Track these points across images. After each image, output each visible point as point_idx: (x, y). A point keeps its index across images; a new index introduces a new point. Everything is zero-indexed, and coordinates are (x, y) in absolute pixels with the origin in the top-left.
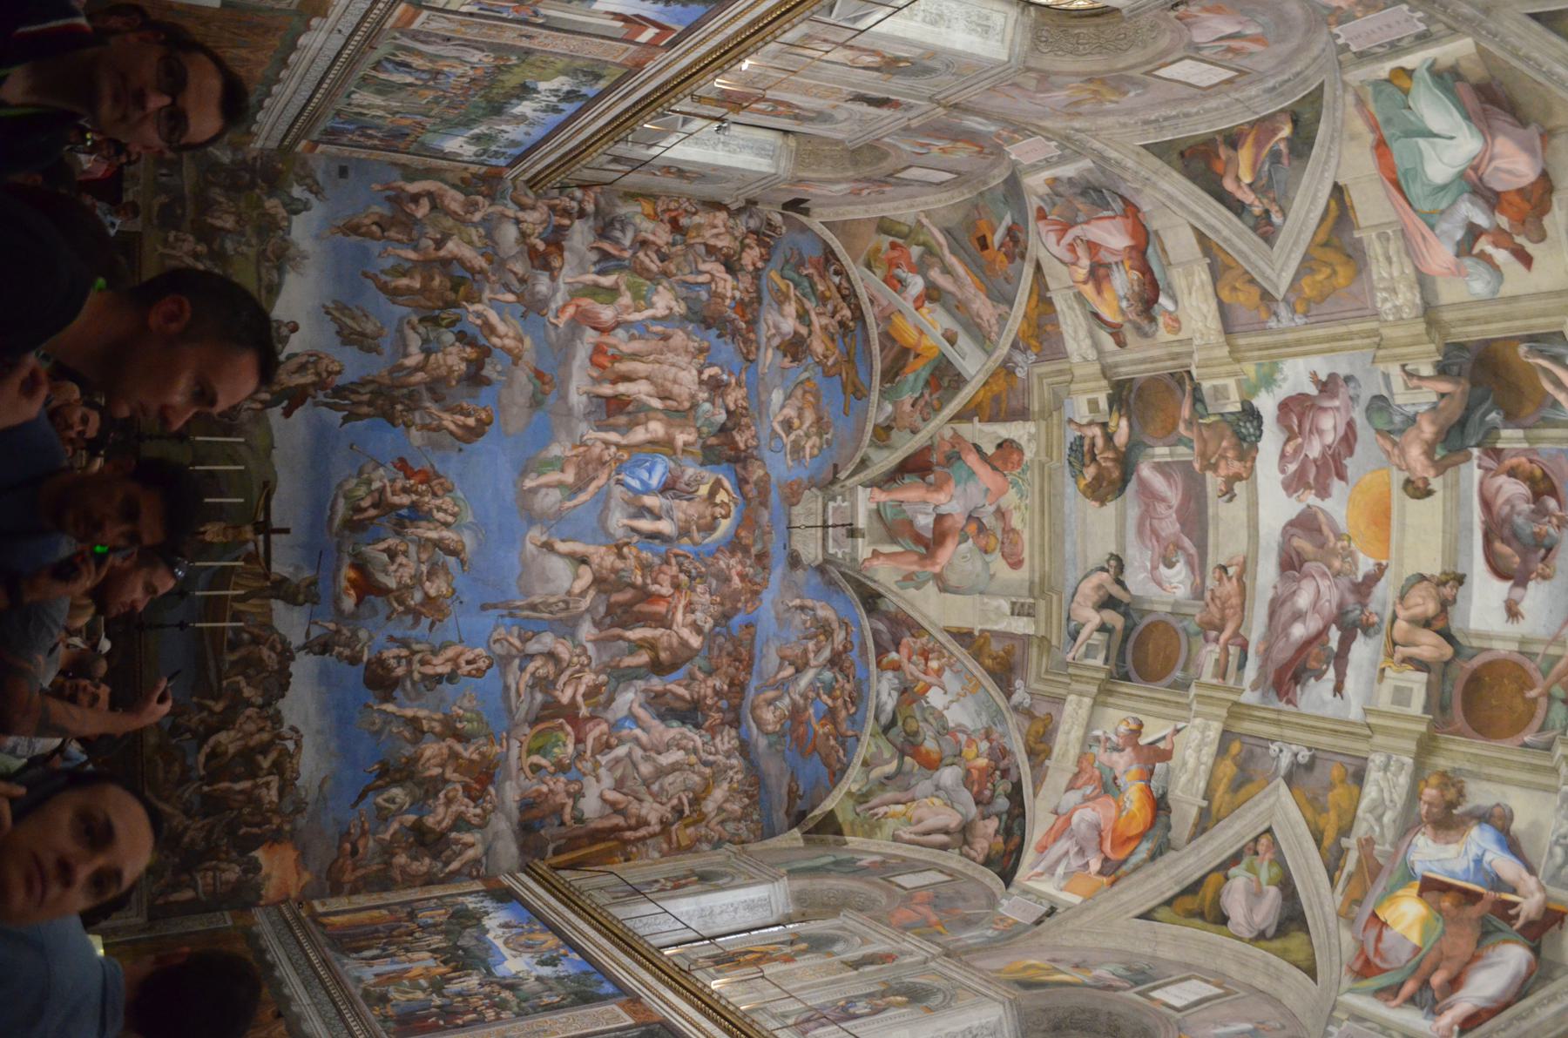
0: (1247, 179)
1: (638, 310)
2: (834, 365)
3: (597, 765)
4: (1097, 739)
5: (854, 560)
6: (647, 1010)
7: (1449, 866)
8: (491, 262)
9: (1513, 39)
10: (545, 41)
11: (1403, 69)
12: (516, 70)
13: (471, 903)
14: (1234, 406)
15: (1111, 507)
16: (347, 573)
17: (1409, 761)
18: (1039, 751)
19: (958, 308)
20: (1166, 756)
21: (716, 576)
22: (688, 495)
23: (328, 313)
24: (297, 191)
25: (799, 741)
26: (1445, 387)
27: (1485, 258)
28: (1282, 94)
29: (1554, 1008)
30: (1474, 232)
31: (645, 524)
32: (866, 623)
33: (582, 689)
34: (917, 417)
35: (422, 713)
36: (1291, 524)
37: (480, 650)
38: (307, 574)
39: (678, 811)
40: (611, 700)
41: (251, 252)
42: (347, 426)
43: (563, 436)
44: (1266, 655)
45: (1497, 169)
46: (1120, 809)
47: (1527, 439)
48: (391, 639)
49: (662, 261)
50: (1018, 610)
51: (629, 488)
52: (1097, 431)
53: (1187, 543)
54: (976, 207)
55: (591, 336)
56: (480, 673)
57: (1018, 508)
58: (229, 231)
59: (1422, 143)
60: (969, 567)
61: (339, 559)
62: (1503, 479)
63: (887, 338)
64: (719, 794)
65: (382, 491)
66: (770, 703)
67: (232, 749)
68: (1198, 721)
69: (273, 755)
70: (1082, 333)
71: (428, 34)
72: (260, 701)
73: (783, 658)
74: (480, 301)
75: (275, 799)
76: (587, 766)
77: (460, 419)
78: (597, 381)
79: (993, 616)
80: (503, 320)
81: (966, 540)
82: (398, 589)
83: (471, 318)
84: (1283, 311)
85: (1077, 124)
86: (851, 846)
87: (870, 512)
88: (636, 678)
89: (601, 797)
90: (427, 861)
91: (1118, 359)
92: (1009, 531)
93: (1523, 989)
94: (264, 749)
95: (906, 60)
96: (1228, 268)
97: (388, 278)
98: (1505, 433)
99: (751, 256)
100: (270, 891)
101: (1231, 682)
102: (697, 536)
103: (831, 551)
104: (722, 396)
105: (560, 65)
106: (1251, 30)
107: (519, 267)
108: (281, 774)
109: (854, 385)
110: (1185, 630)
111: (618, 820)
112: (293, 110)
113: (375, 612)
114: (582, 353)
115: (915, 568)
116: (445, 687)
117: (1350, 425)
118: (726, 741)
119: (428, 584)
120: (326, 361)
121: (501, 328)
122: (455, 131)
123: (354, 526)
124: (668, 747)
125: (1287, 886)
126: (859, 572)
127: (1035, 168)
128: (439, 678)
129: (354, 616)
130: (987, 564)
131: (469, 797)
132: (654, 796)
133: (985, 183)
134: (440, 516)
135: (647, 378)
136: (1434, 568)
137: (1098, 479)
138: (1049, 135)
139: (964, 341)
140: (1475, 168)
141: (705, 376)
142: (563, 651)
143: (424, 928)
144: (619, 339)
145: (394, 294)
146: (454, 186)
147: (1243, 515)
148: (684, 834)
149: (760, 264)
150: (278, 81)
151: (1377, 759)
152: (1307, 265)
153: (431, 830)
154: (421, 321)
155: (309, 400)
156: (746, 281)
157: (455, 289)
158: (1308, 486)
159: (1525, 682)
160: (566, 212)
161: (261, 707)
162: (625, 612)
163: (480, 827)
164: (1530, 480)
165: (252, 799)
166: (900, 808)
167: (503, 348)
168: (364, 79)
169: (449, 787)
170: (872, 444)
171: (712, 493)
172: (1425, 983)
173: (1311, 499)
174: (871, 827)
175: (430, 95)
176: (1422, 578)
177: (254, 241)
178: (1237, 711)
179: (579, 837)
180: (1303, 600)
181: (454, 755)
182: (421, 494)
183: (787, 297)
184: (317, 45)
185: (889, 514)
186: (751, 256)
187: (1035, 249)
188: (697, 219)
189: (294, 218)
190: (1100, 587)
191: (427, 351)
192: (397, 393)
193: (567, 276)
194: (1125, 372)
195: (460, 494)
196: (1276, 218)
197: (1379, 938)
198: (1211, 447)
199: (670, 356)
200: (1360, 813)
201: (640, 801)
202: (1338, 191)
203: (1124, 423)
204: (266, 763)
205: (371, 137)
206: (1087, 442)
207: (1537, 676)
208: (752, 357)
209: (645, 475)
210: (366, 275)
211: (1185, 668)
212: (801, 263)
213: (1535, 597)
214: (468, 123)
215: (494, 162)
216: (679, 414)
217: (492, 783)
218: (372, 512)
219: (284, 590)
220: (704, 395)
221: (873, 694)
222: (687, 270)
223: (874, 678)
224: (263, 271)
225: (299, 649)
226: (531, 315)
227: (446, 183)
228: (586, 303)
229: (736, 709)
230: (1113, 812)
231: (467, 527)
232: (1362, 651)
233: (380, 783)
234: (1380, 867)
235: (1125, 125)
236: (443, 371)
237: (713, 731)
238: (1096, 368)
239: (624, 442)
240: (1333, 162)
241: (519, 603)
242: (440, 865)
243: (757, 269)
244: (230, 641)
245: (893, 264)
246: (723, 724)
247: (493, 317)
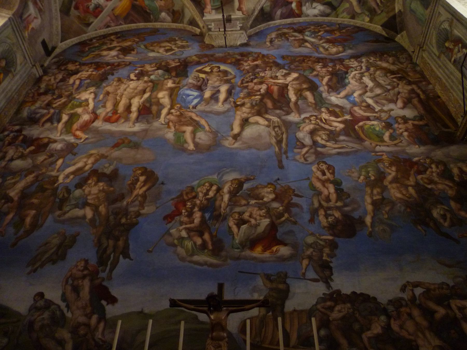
1: (88, 105)
2: (138, 38)
3: (381, 111)
5: (243, 19)
16: (258, 252)
21: (254, 70)
23: (35, 271)
25: (346, 40)
31: (222, 96)
32: (278, 22)
33: (333, 118)
35: (368, 200)
37: (314, 168)
38: (260, 282)
39: (400, 79)
40: (337, 106)
42: (132, 255)
48: (312, 221)
49: (62, 97)
55: (97, 124)
61: (246, 258)
63: (127, 19)
64: (385, 65)
65: (189, 230)
69: (432, 305)
72: (383, 318)
73: (300, 46)
74: (58, 177)
80: (74, 164)
82: (270, 217)
83: (68, 181)
86: (401, 8)
88: (321, 96)
89: (403, 108)
97: (22, 230)
99: (71, 67)
102: (230, 77)
104: (147, 72)
107: (41, 158)
111: (415, 101)
114: (108, 127)
116: (345, 186)
119: (265, 199)
120: (74, 271)
121: (80, 165)
126: (249, 16)
129: (295, 246)
131: (425, 171)
132: (394, 88)
134: (211, 194)
135: (130, 99)
141: (135, 78)
142: (309, 127)
145: (35, 226)
149: (77, 64)
154: (60, 208)
155: (105, 283)
157: (43, 190)
160: (16, 138)
161: (389, 317)
162: (279, 102)
167: (93, 164)
169: (421, 182)
170: (182, 22)
171: (205, 72)
182: (194, 205)
186: (71, 67)
188: (43, 86)
193: (55, 136)
201: (399, 93)
204: (441, 311)
208: (128, 63)
218: (207, 236)
220: (146, 78)
221: (316, 19)
222: (71, 88)
226: (75, 150)
228: (75, 126)
229: (332, 61)
231: (221, 178)
233: (431, 224)
236: (102, 195)
237: (348, 68)
239: (169, 107)
241: (277, 149)
245: (87, 10)
246: (343, 65)
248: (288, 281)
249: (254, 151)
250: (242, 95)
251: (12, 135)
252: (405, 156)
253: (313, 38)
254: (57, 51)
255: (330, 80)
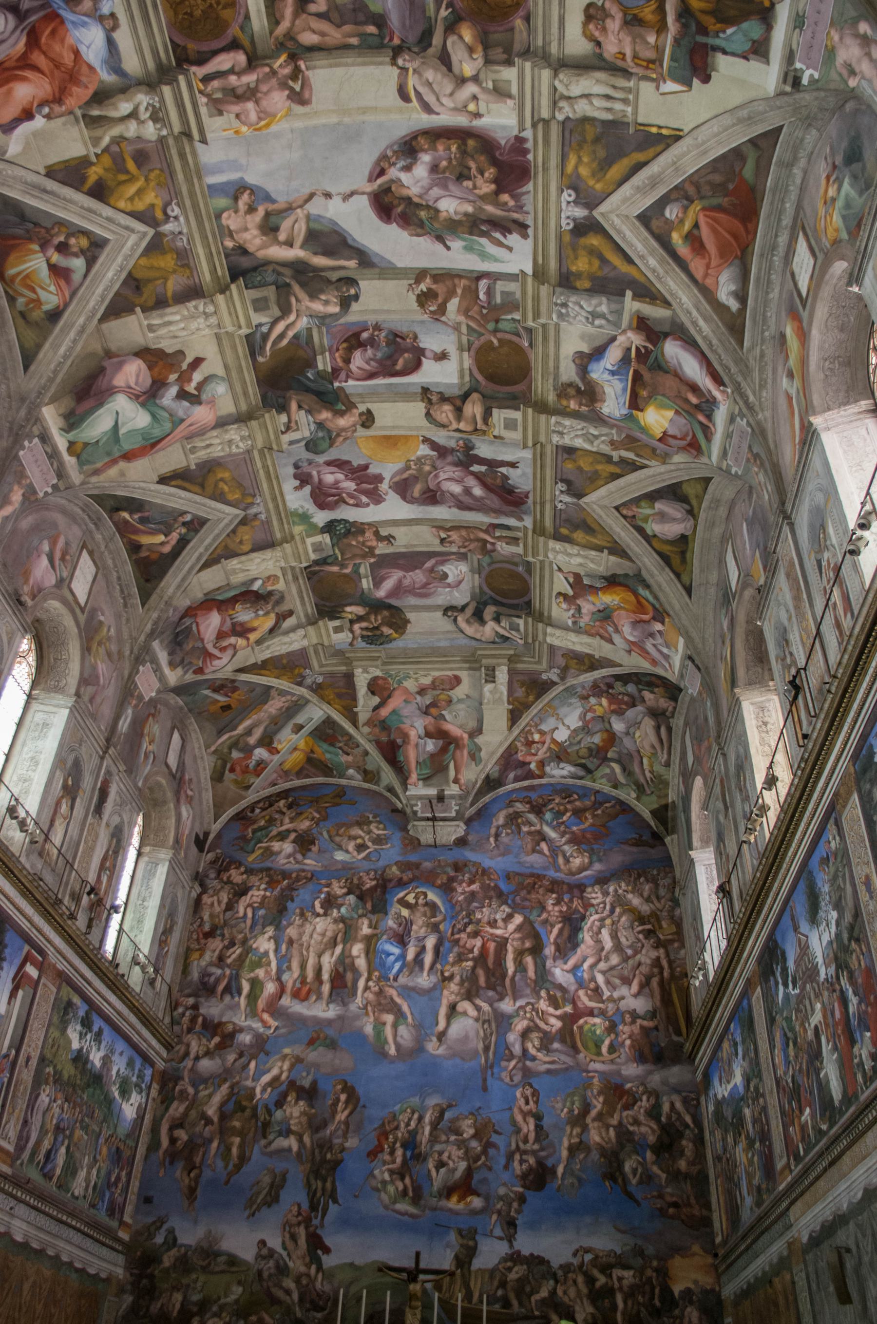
0: (162, 538)
3: (611, 999)
4: (574, 623)
5: (461, 797)
6: (754, 972)
7: (619, 392)
8: (225, 1080)
9: (43, 381)
10: (33, 1046)
11: (69, 449)
12: (59, 1067)
13: (711, 1108)
14: (327, 538)
15: (410, 616)
16: (453, 1203)
17: (553, 419)
18: (590, 663)
19: (276, 724)
20: (577, 576)
22: (407, 925)
23: (253, 1215)
24: (159, 1239)
26: (294, 406)
27: (200, 387)
28: (99, 519)
29: (701, 322)
30: (183, 395)
31: (428, 958)
33: (551, 1010)
34: (356, 751)
35: (566, 1143)
36: (404, 498)
37: (518, 1094)
38: (453, 1237)
39: (648, 934)
40: (560, 987)
41: (202, 1278)
43: (358, 1023)
44: (498, 512)
45: (136, 383)
46: (620, 608)
47: (323, 353)
48: (506, 1167)
50: (491, 678)
51: (400, 971)
52: (356, 627)
53: (428, 564)
54: (200, 713)
55: (286, 1001)
56: (535, 1093)
57: (416, 679)
58: (185, 1298)
59: (122, 431)
60: (462, 713)
61: (442, 1209)
62: (353, 367)
63: (300, 774)
64: (636, 901)
65: (391, 1172)
66: (567, 861)
67: (590, 1309)
68: (551, 556)
69: (596, 1273)
70: (286, 639)
71: (20, 1138)
72: (552, 1282)
73: (534, 851)
74: (254, 1089)
75: (631, 1273)
76: (611, 1007)
77: (341, 1106)
78: (319, 997)
79: (497, 696)
80: (269, 1071)
81: (443, 717)
83: (266, 1096)
84: (253, 511)
85: (127, 653)
87: (427, 785)
88: (544, 966)
89: (635, 996)
90: (684, 1142)
91: (302, 615)
92: (434, 686)
93: (690, 343)
94: (591, 1281)
95: (65, 781)
96: (226, 547)
98: (320, 366)
99: (236, 876)
100: (707, 1281)
101: (520, 534)
102: (439, 918)
103: (454, 814)
104: (336, 897)
105: (57, 1034)
106: (46, 547)
107: (231, 1057)
108: (611, 1266)
109: (335, 797)
110: (489, 565)
111: (655, 982)
112: (88, 1244)
113: (485, 1181)
114: (298, 1008)
115: (465, 752)
116: (546, 1122)
117: (329, 463)
118: (595, 895)
121: (275, 1072)
122: (116, 1111)
123: (417, 1198)
124: (598, 941)
125: (652, 497)
127: (162, 678)
128: (539, 1128)
129: (487, 1199)
130: (460, 701)
131: (634, 1104)
132: (636, 952)
133: (181, 708)
134: (413, 1124)
135: (320, 956)
136: (420, 407)
137: (390, 625)
138: (134, 671)
139: (300, 719)
140: (137, 397)
141: (321, 911)
142: (521, 1025)
143: (725, 1150)
144: (290, 979)
145: (243, 1159)
146: (167, 1109)
147: (403, 529)
148: (667, 929)
149: (242, 869)
150: (57, 1257)
151: (556, 439)
152: (220, 497)
153: (659, 1138)
154: (265, 1137)
155: (319, 1231)
156: (254, 880)
157: (243, 1109)
158: (376, 489)
159: (487, 347)
161: (557, 1282)
163: (657, 1097)
164: (350, 350)
165: (630, 1294)
166: (645, 761)
168: (59, 1187)
170: (377, 783)
171: (407, 905)
172: (697, 407)
173: (384, 486)
174: (661, 783)
175: (78, 1133)
176: (428, 415)
177: (194, 1276)
178: (539, 530)
179: (668, 1018)
180: (456, 489)
181: (600, 1117)
183: (267, 849)
184: (24, 1226)
185: (426, 771)
187: (227, 673)
188: (206, 918)
189: (179, 1241)
190: (468, 622)
191: (287, 1132)
192: (318, 1158)
193: (240, 1019)
194: (310, 609)
195: (397, 1108)
196: (188, 518)
197: (674, 437)
198: (358, 552)
199: (305, 938)
200: (594, 449)
202: (163, 480)
203: (348, 609)
204: (602, 1280)
205: (118, 1178)
206: (365, 633)
207: (483, 339)
209: (392, 958)
210: (227, 1182)
211: (516, 564)
212: (244, 838)
213: (430, 342)
214: (109, 1101)
215: (148, 1078)
216: (348, 932)
217: (622, 1085)
218: (407, 1181)
219: (465, 1259)
220: (335, 913)
221: (564, 781)
223: (552, 780)
224: (217, 1269)
225: (511, 1246)
226: (268, 1047)
227: (163, 1116)
228: (261, 1003)
230: (623, 612)
232: (484, 450)
234: (628, 436)
235: (128, 620)
236: (304, 1119)
237: (587, 905)
238: (310, 629)
239: (365, 975)
240: (143, 485)
242: (687, 1132)
243: (245, 872)
244: (504, 1307)
245: (246, 771)
246: (582, 898)
247: (266, 1078)
248: (477, 1238)
249: (458, 1061)
250: (451, 959)
251: (188, 1013)
252: (619, 1081)
253: (554, 828)
254: (212, 836)
255: (561, 931)
